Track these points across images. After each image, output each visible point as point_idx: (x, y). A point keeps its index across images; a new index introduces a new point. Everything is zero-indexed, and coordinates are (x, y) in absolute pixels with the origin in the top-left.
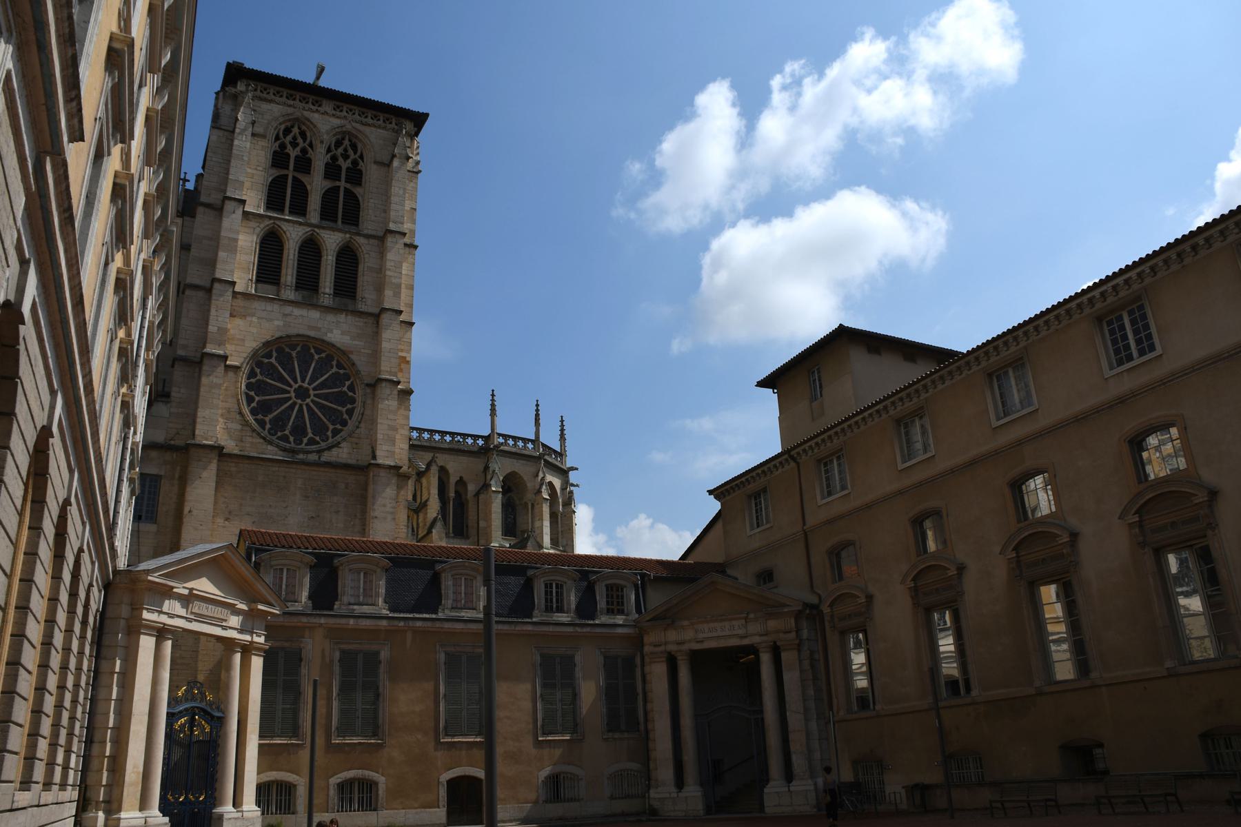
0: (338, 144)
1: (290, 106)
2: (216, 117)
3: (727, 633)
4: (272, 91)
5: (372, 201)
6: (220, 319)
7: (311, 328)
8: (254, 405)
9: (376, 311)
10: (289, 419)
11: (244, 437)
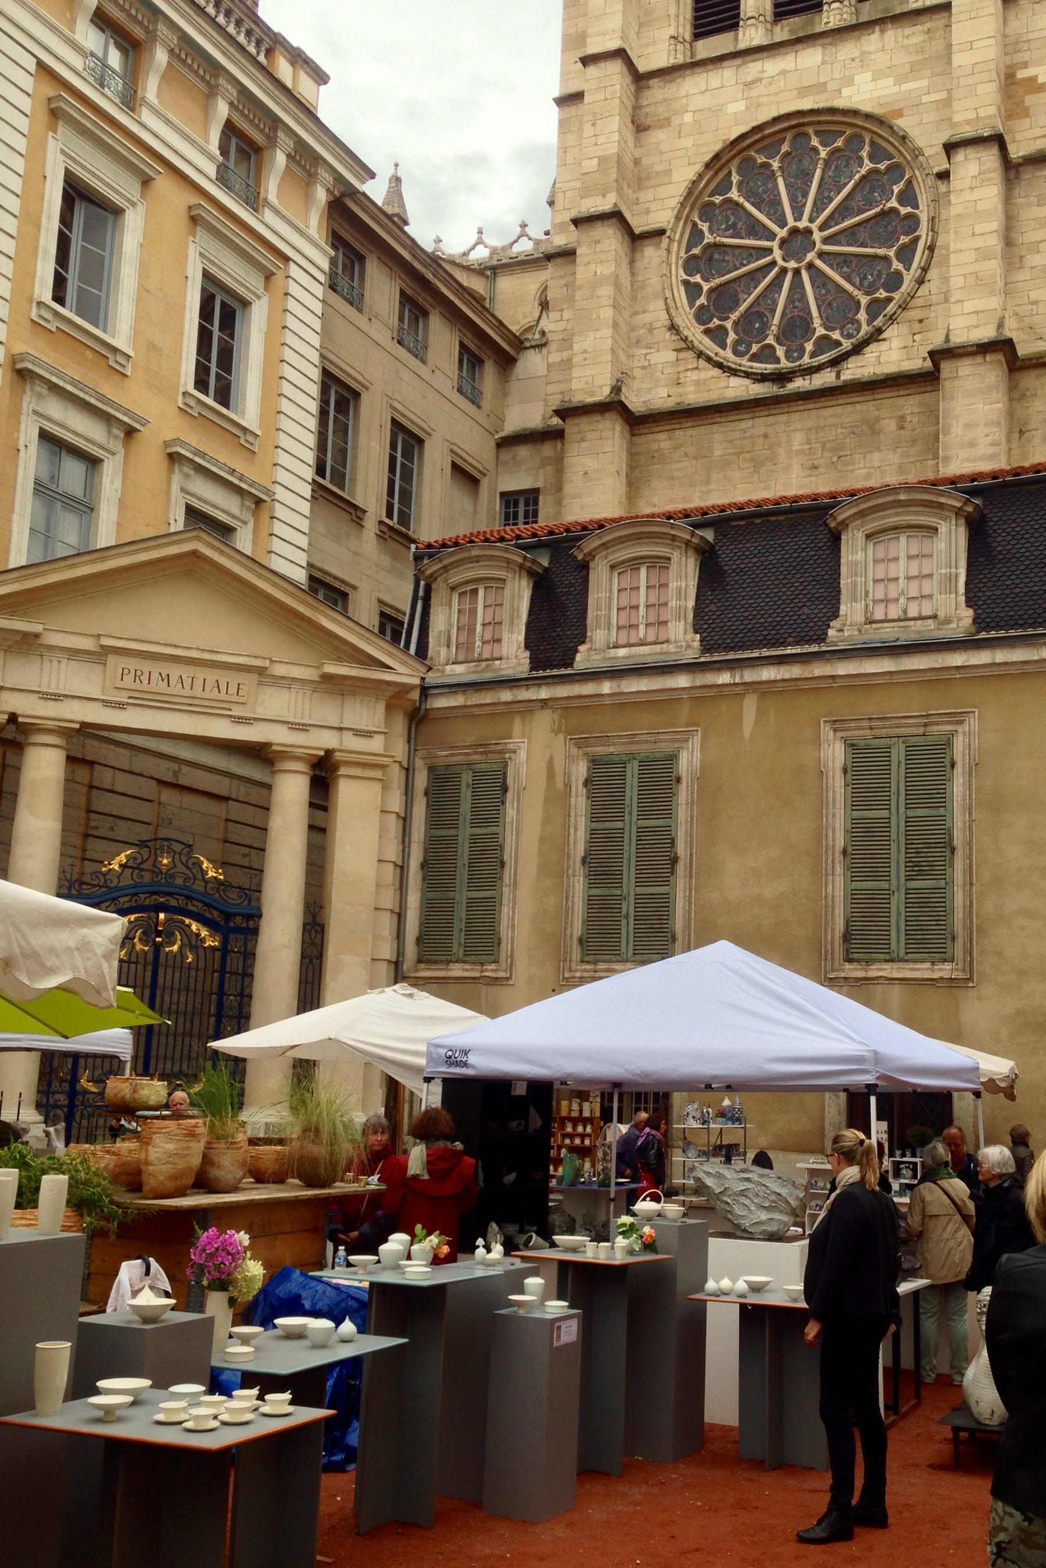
7: (803, 91)
8: (702, 300)
10: (773, 311)
11: (681, 375)
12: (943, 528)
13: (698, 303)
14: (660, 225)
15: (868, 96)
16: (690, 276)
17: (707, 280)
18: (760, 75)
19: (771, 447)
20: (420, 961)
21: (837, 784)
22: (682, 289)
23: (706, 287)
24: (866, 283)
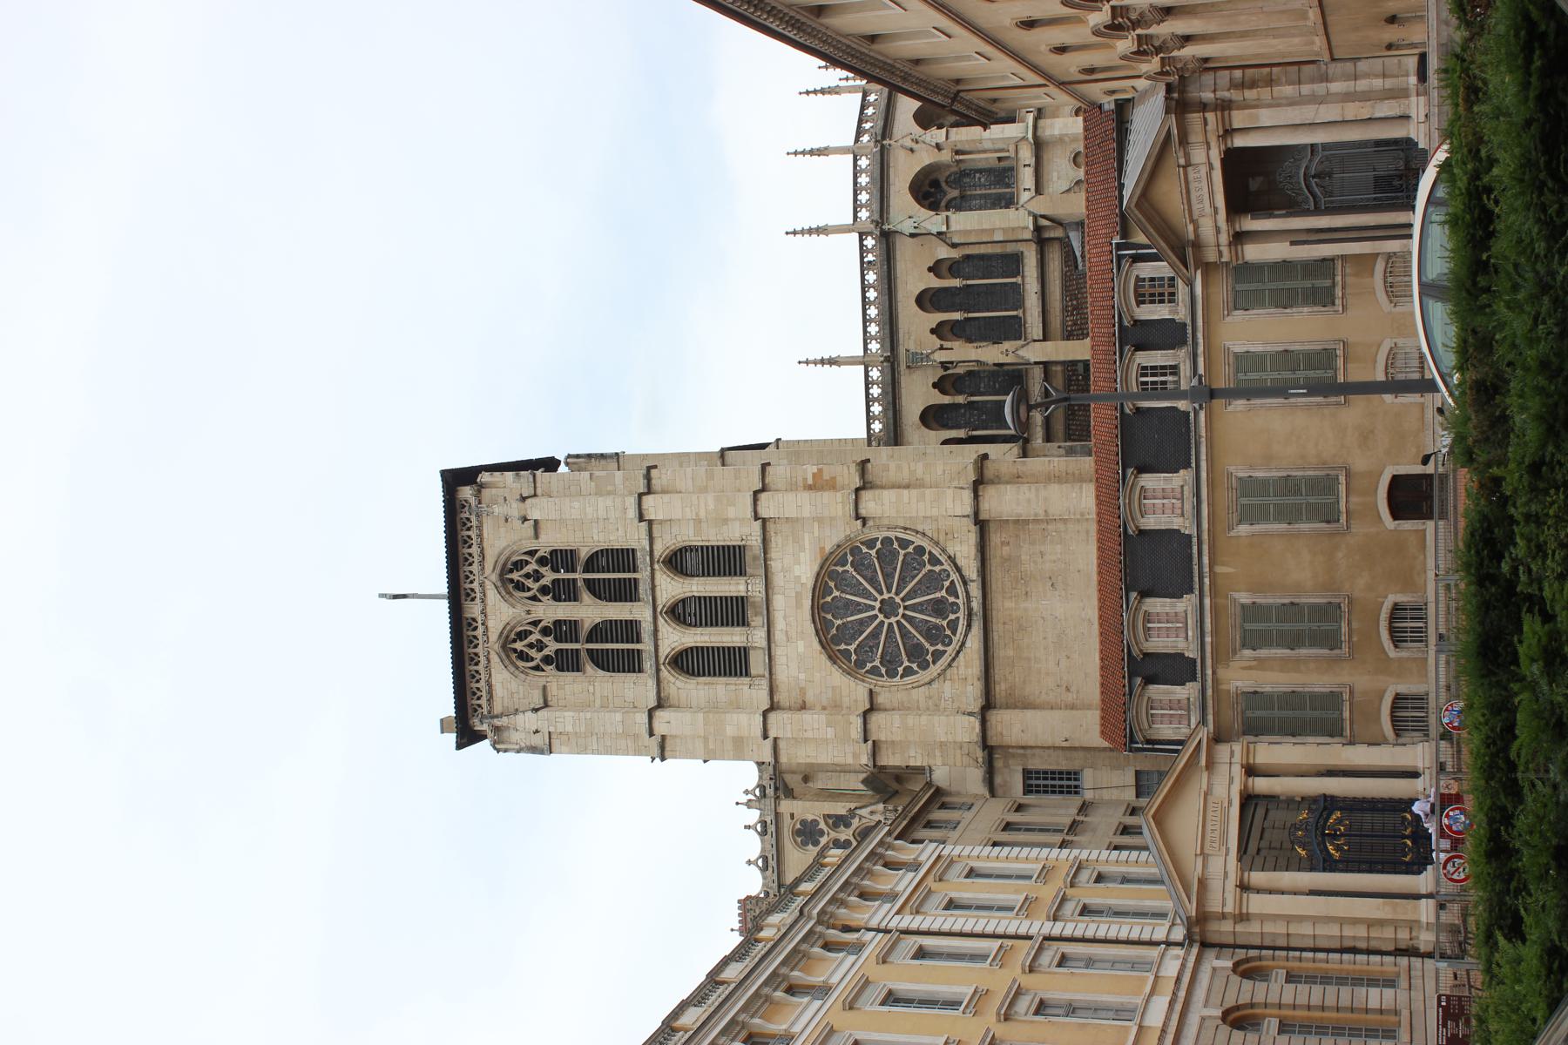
0: (520, 587)
1: (489, 660)
2: (533, 750)
3: (1204, 184)
4: (475, 685)
5: (596, 538)
6: (816, 726)
7: (799, 605)
8: (914, 666)
10: (927, 621)
12: (1142, 483)
13: (916, 668)
19: (1012, 620)
20: (1341, 735)
21: (1257, 528)
22: (905, 679)
23: (906, 664)
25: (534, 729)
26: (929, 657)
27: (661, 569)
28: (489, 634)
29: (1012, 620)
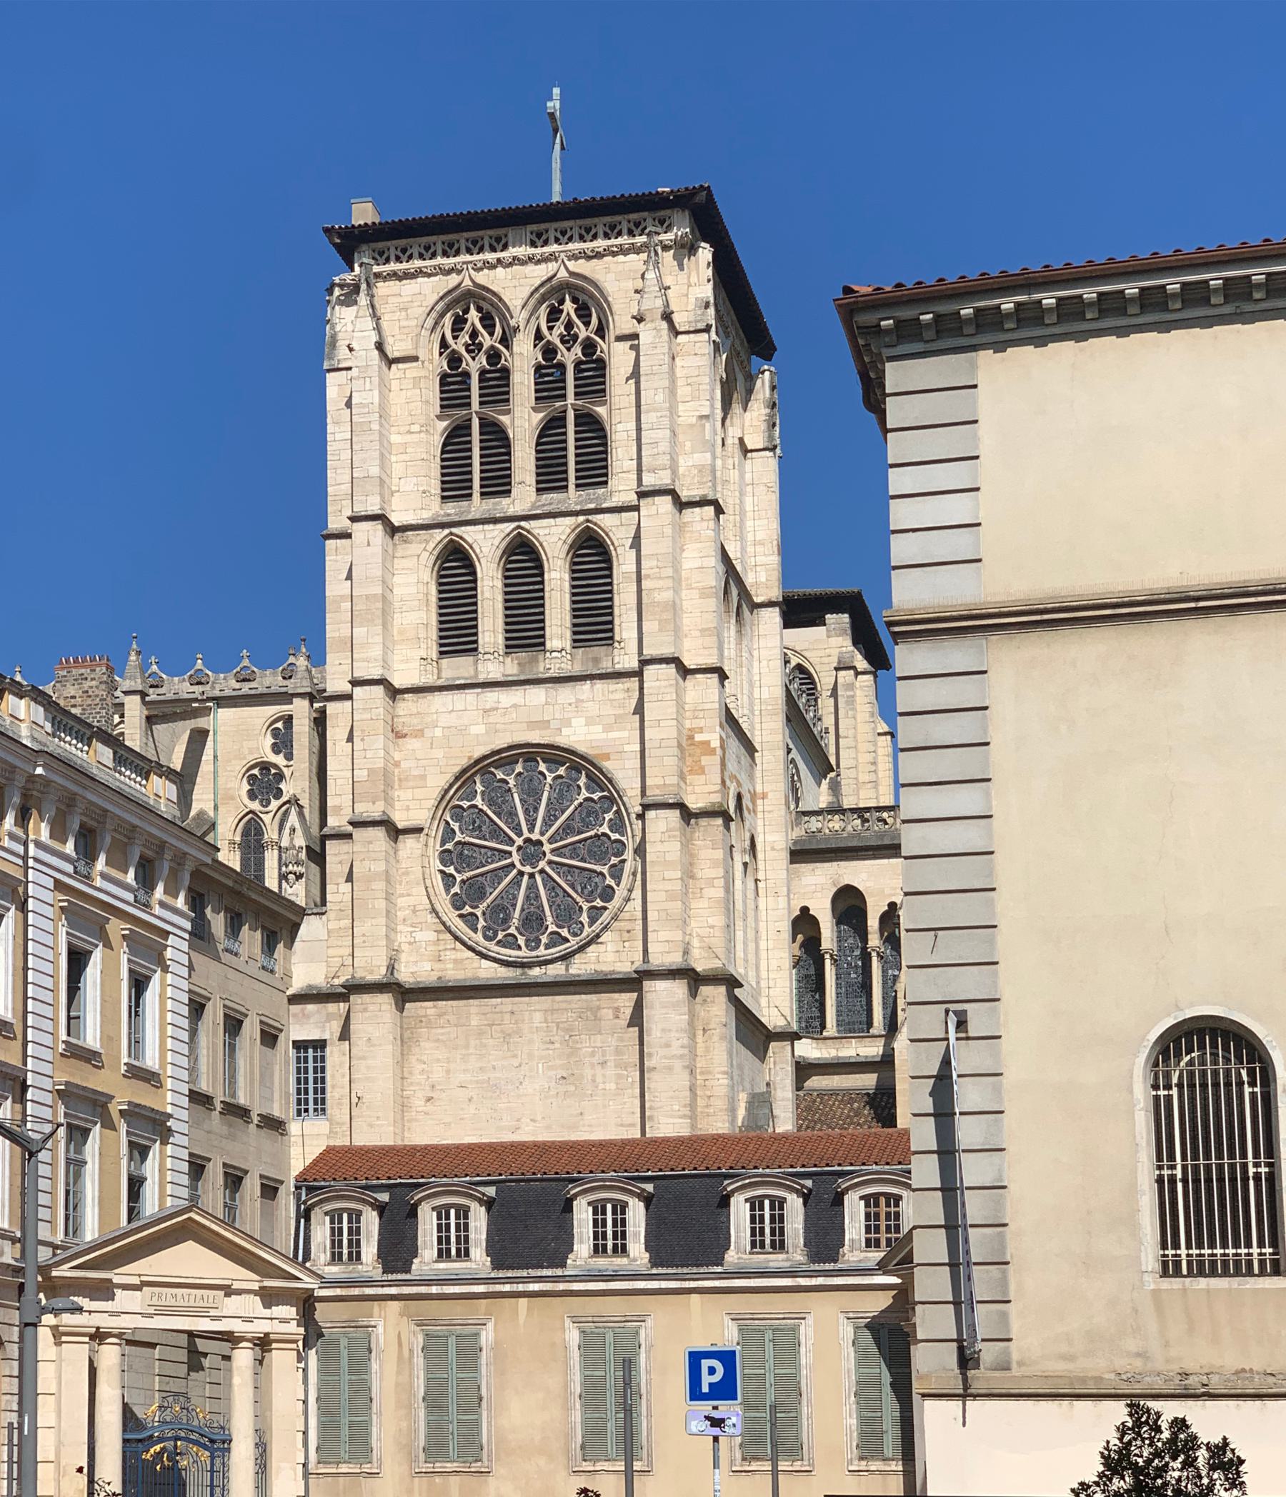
5: (620, 427)
7: (532, 725)
8: (456, 889)
9: (634, 664)
10: (514, 905)
11: (442, 953)
13: (453, 891)
14: (419, 822)
15: (582, 738)
16: (445, 866)
17: (459, 872)
18: (496, 705)
19: (516, 1023)
22: (439, 876)
23: (459, 878)
24: (586, 892)
25: (354, 345)
26: (467, 909)
27: (579, 525)
28: (486, 271)
29: (516, 1023)
